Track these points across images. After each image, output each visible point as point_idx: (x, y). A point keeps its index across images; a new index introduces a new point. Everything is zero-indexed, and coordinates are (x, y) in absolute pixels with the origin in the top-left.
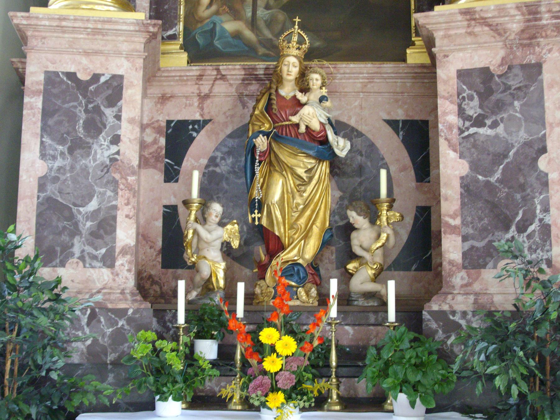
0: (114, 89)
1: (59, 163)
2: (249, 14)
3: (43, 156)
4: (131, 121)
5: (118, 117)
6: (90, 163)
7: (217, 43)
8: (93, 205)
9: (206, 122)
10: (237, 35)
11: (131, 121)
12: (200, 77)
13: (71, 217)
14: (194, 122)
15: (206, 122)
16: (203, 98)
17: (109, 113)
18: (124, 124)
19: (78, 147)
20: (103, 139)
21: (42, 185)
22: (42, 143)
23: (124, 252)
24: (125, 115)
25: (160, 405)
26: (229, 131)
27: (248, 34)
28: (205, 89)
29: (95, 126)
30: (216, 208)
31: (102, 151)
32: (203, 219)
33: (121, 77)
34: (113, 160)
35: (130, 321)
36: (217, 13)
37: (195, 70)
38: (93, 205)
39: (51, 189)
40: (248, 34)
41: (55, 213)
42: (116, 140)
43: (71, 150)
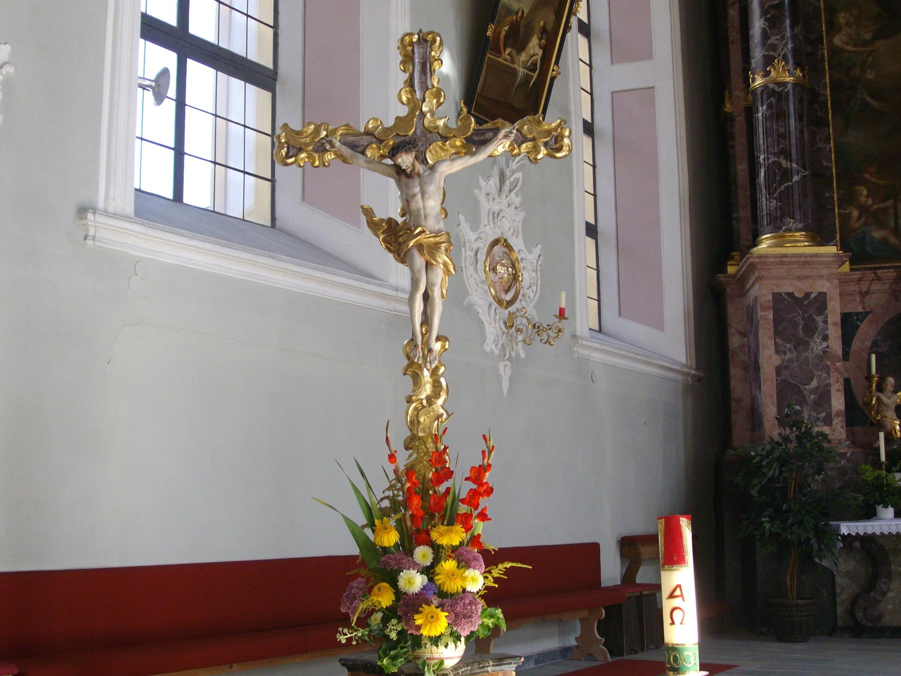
0: (821, 302)
1: (789, 356)
2: (893, 224)
3: (777, 352)
4: (835, 324)
5: (826, 322)
6: (809, 355)
7: (868, 248)
8: (814, 384)
9: (867, 313)
10: (884, 241)
11: (835, 324)
12: (860, 280)
13: (800, 392)
14: (858, 314)
15: (867, 313)
16: (863, 295)
17: (819, 319)
18: (830, 327)
19: (801, 345)
20: (817, 339)
21: (778, 370)
22: (776, 343)
23: (837, 415)
24: (830, 321)
25: (880, 509)
26: (887, 319)
27: (893, 239)
28: (864, 288)
29: (810, 329)
30: (891, 380)
31: (817, 346)
32: (880, 389)
33: (824, 294)
34: (825, 352)
35: (848, 460)
36: (866, 224)
37: (857, 275)
38: (814, 384)
39: (785, 374)
40: (893, 239)
41: (787, 391)
42: (825, 338)
43: (796, 347)
